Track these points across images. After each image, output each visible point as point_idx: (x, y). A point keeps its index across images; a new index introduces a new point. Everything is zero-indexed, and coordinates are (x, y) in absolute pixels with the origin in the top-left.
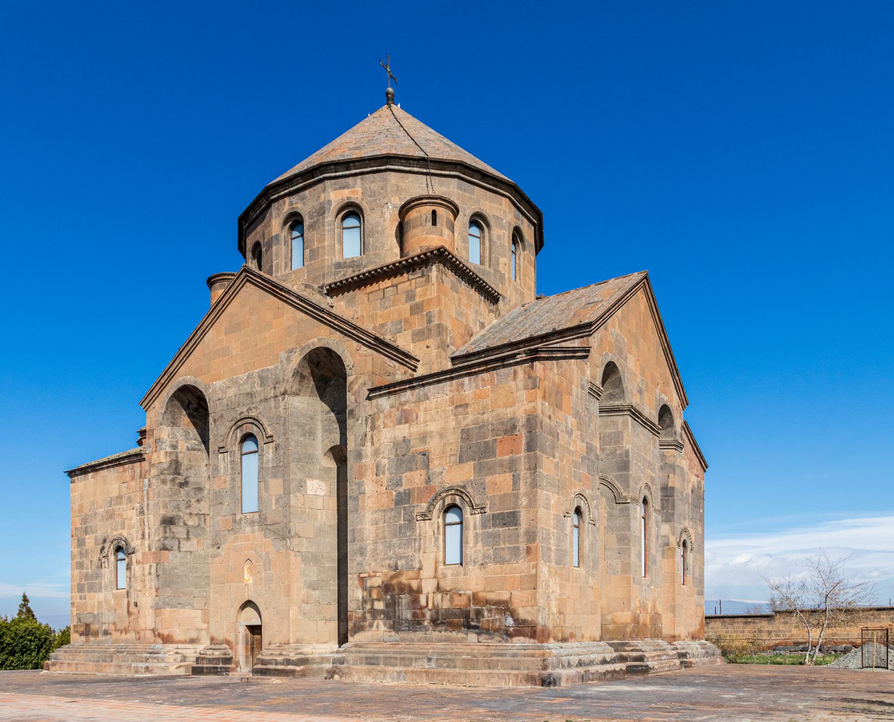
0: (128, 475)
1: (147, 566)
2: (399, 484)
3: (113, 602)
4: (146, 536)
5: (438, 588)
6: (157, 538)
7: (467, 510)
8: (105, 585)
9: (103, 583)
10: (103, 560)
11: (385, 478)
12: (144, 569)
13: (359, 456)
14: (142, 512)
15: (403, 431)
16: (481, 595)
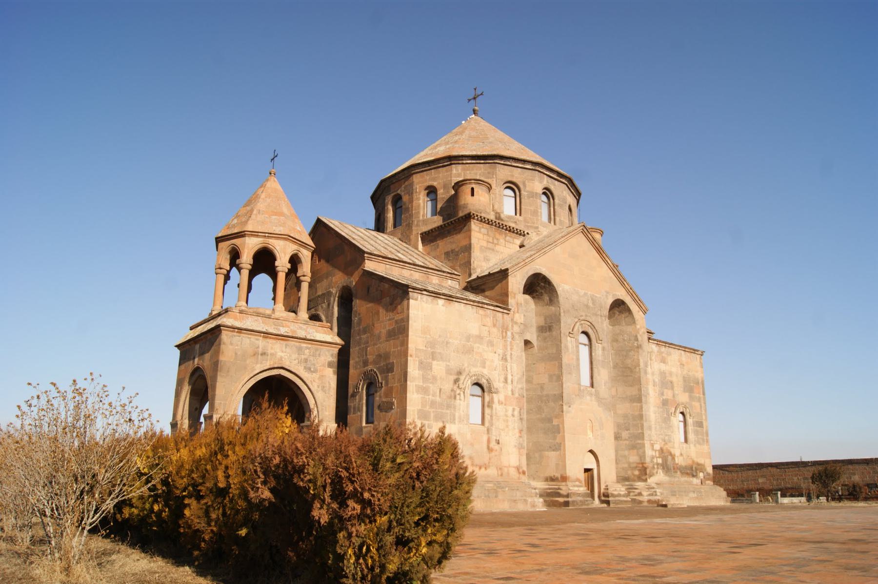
0: (489, 321)
1: (510, 409)
2: (662, 394)
3: (469, 436)
4: (509, 381)
5: (681, 454)
6: (520, 386)
7: (688, 416)
8: (460, 418)
9: (457, 415)
10: (458, 392)
11: (657, 388)
12: (506, 411)
13: (646, 373)
14: (504, 359)
15: (663, 367)
16: (696, 460)
